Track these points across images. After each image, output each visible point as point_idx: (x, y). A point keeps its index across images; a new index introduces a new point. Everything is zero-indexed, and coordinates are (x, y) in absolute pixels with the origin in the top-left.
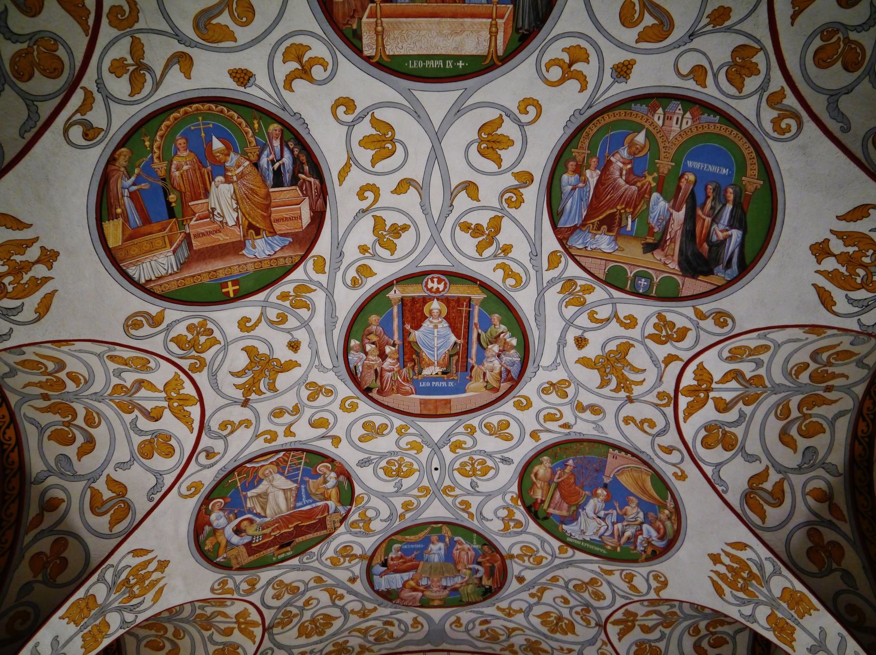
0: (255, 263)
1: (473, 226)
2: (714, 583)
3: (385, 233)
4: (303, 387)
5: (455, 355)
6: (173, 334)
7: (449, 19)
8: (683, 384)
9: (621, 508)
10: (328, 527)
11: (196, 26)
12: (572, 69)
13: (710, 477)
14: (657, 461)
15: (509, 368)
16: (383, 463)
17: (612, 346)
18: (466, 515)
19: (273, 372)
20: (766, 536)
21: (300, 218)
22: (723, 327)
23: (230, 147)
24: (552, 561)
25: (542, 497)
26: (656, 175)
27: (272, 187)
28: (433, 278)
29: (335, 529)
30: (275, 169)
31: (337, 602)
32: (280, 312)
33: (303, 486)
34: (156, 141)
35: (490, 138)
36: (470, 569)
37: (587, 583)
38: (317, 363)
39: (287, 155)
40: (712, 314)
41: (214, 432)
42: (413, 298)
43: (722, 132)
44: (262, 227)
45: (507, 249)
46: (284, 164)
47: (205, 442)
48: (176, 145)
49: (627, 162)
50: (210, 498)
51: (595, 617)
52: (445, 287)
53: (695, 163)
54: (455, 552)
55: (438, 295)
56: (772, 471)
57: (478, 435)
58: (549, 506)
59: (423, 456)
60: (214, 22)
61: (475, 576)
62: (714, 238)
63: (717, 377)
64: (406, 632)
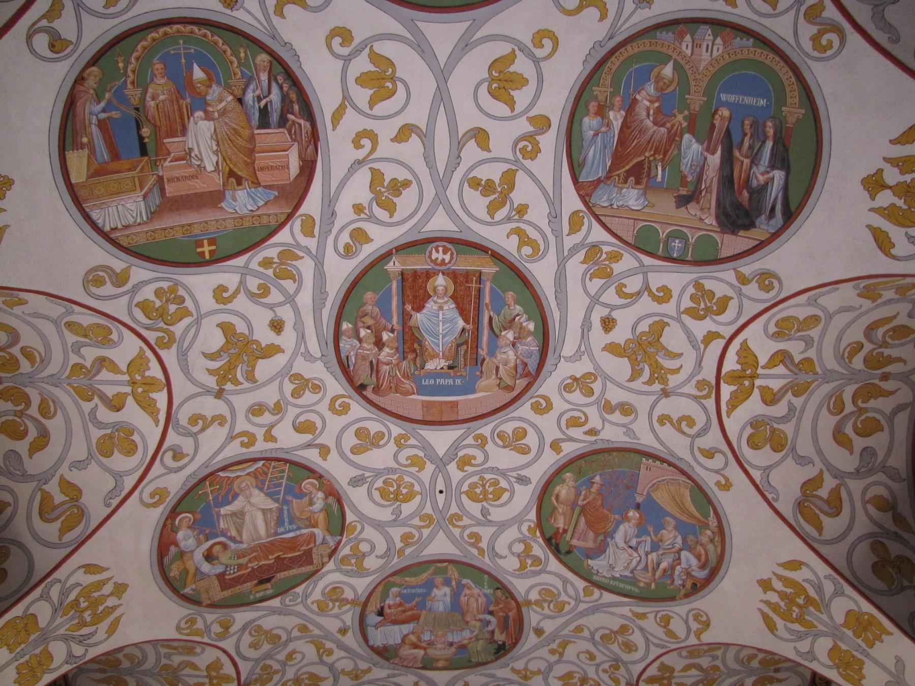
0: (234, 219)
1: (483, 183)
2: (765, 617)
3: (383, 190)
4: (287, 380)
5: (463, 344)
6: (139, 298)
8: (725, 369)
10: (315, 561)
13: (758, 483)
14: (698, 469)
15: (525, 360)
16: (379, 483)
17: (644, 327)
18: (475, 552)
20: (823, 550)
21: (288, 168)
22: (768, 292)
23: (212, 78)
24: (576, 607)
26: (686, 113)
29: (323, 565)
30: (262, 107)
31: (325, 658)
32: (262, 282)
33: (285, 507)
34: (131, 63)
35: (502, 76)
36: (481, 620)
38: (303, 349)
39: (275, 90)
40: (755, 276)
41: (183, 427)
42: (415, 272)
43: (757, 57)
44: (244, 176)
45: (522, 210)
46: (271, 101)
47: (172, 438)
49: (654, 99)
50: (178, 510)
52: (452, 258)
53: (729, 96)
55: (443, 268)
56: (826, 475)
57: (490, 447)
62: (755, 184)
63: (763, 361)
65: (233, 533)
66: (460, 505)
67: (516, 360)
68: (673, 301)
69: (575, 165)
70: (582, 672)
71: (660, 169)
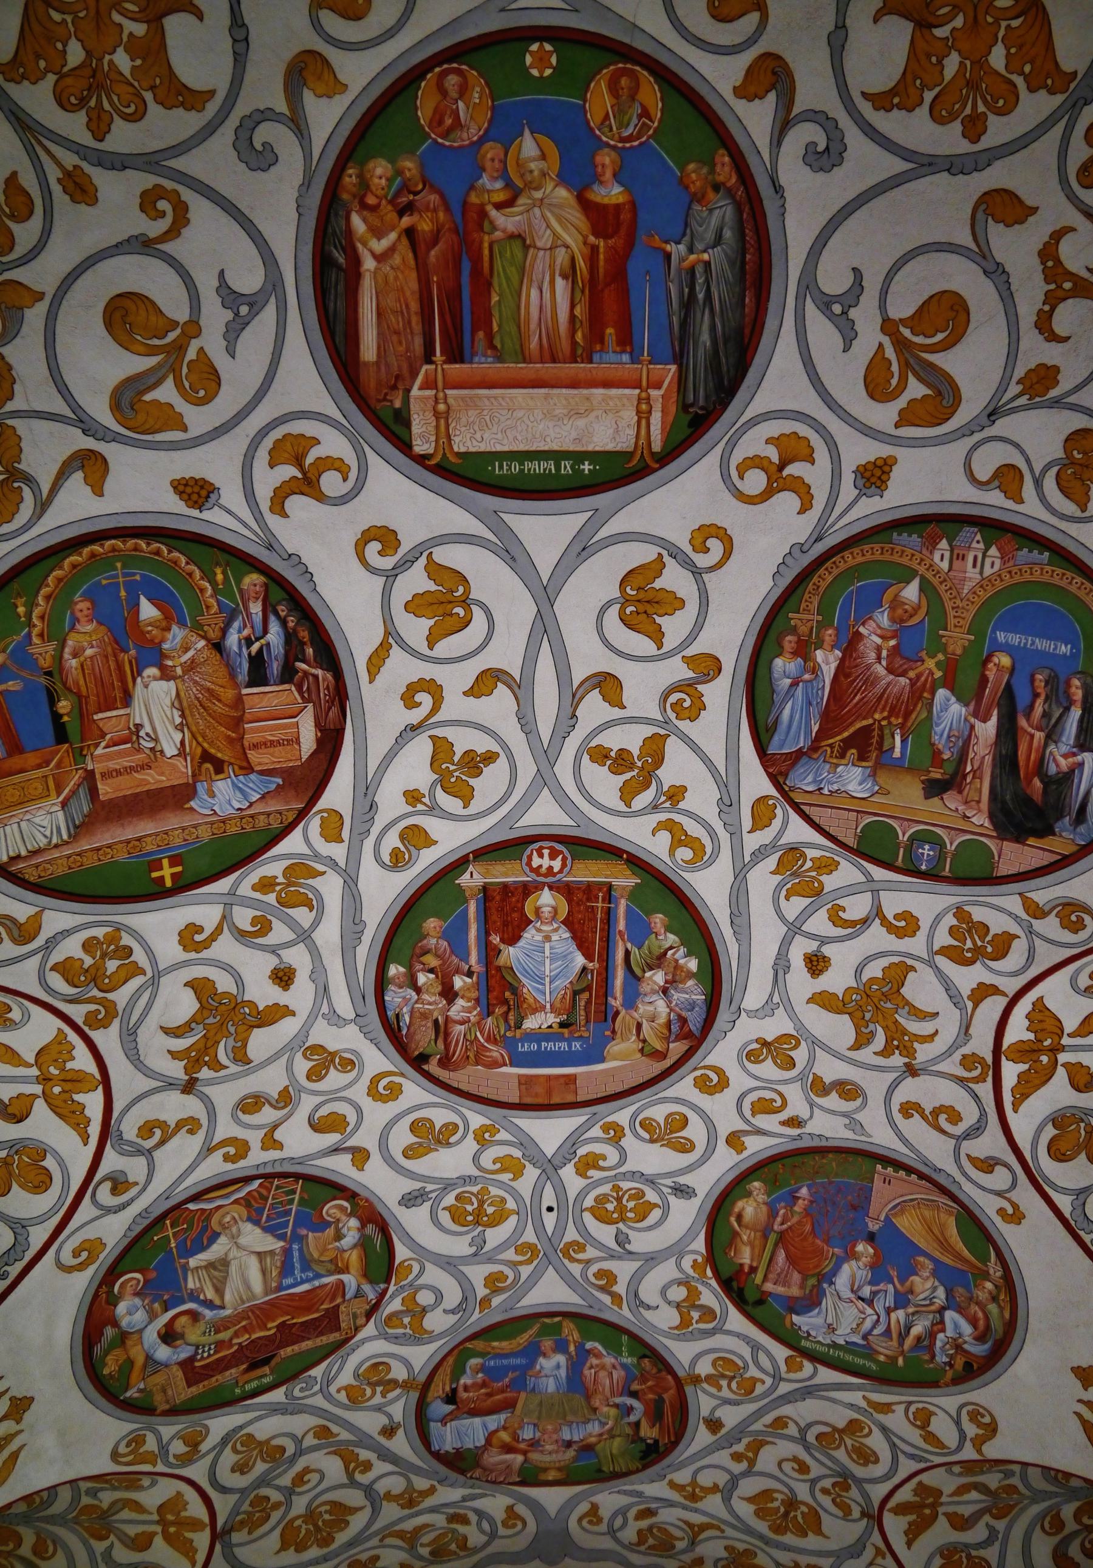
0: (212, 823)
1: (613, 754)
3: (452, 768)
4: (299, 1055)
5: (583, 991)
6: (57, 956)
7: (564, 391)
8: (1009, 1039)
9: (902, 1281)
10: (343, 1325)
11: (116, 405)
12: (785, 473)
13: (1067, 1215)
14: (967, 1187)
15: (684, 1014)
16: (450, 1200)
17: (874, 970)
18: (606, 1299)
19: (242, 1028)
21: (298, 743)
22: (1076, 932)
23: (170, 616)
24: (774, 1388)
25: (752, 1260)
26: (941, 657)
27: (246, 687)
28: (542, 848)
29: (357, 1329)
30: (253, 654)
31: (358, 1477)
32: (259, 913)
33: (295, 1246)
34: (38, 605)
35: (642, 595)
36: (617, 1406)
38: (325, 1009)
39: (274, 627)
40: (1054, 908)
41: (130, 1143)
42: (505, 886)
43: (1056, 580)
44: (226, 758)
45: (676, 794)
46: (268, 644)
47: (111, 1161)
48: (73, 613)
49: (889, 634)
50: (119, 1269)
51: (860, 1499)
52: (564, 865)
53: (1010, 636)
54: (586, 1372)
55: (550, 879)
57: (628, 1141)
58: (765, 1278)
59: (526, 1184)
60: (148, 397)
61: (626, 1420)
62: (1052, 769)
64: (493, 1535)
65: (210, 1294)
66: (582, 1229)
67: (669, 1014)
68: (922, 935)
69: (762, 731)
70: (786, 1490)
71: (898, 739)
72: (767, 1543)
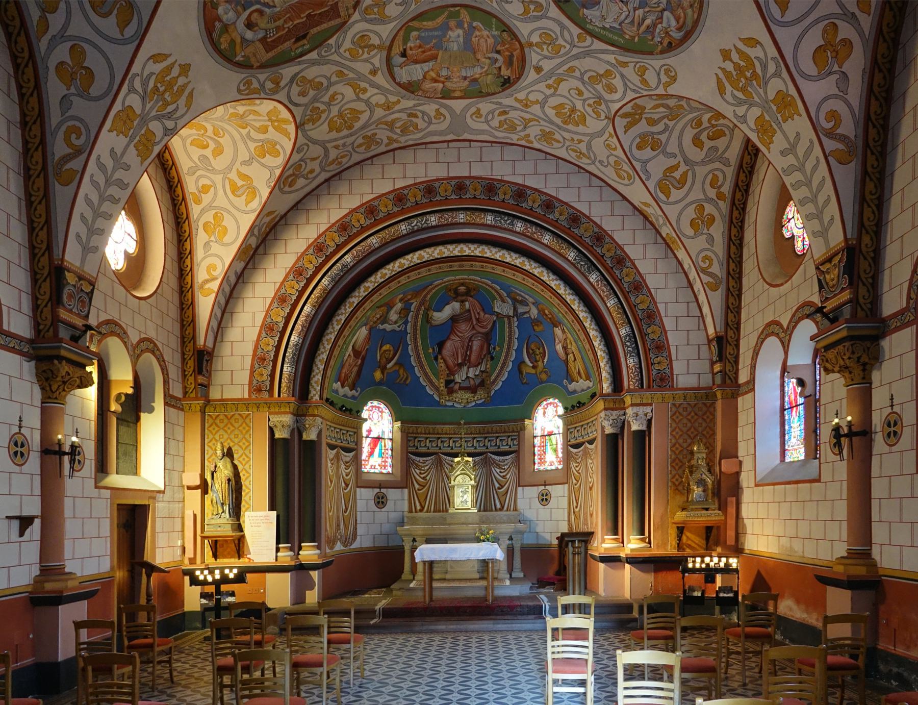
36: (489, 58)
37: (602, 75)
54: (473, 39)
61: (495, 66)
70: (570, 103)
72: (560, 129)
